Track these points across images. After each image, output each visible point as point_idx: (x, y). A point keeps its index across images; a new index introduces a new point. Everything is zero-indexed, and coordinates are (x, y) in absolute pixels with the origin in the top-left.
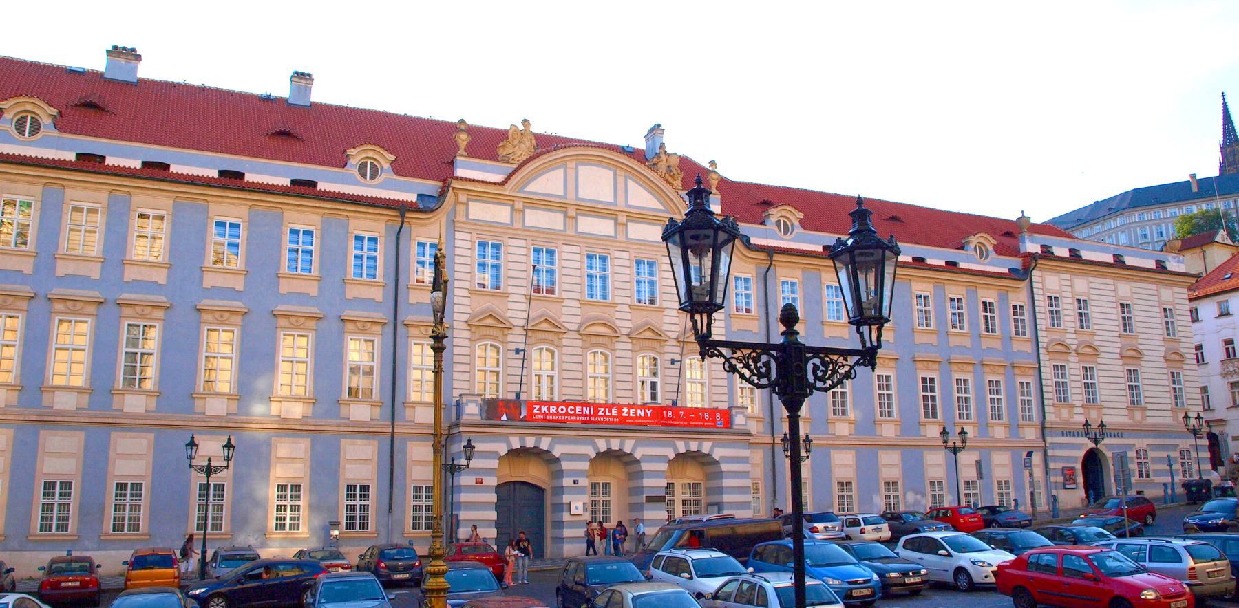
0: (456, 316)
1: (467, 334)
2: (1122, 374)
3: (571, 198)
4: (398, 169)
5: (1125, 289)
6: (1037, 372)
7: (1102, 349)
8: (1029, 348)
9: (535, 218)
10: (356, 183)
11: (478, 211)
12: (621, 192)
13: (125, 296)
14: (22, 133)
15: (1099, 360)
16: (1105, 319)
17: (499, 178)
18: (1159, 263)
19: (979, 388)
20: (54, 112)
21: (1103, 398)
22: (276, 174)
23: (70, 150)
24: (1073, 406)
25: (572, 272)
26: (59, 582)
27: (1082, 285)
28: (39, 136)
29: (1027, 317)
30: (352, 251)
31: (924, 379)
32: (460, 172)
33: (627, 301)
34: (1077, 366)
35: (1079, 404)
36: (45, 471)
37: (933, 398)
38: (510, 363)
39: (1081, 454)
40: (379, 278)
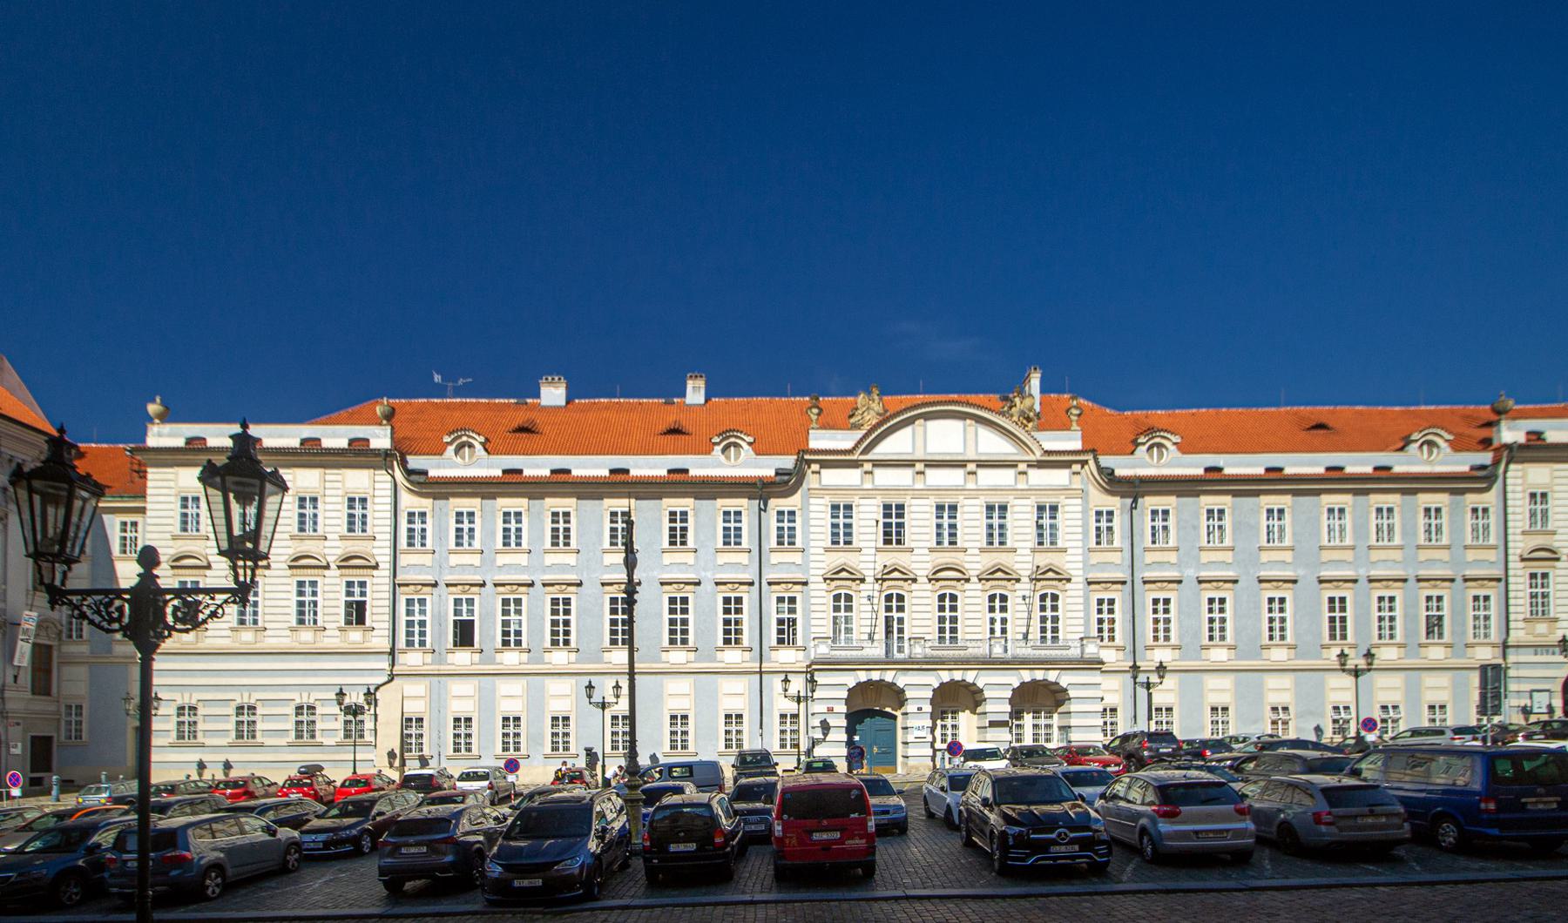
0: (812, 572)
1: (824, 586)
3: (919, 455)
4: (760, 449)
9: (884, 477)
10: (720, 465)
11: (831, 477)
12: (971, 443)
17: (849, 445)
19: (1410, 605)
20: (482, 439)
22: (654, 467)
25: (921, 523)
30: (721, 525)
32: (813, 444)
33: (978, 545)
37: (1343, 619)
38: (863, 608)
40: (745, 544)
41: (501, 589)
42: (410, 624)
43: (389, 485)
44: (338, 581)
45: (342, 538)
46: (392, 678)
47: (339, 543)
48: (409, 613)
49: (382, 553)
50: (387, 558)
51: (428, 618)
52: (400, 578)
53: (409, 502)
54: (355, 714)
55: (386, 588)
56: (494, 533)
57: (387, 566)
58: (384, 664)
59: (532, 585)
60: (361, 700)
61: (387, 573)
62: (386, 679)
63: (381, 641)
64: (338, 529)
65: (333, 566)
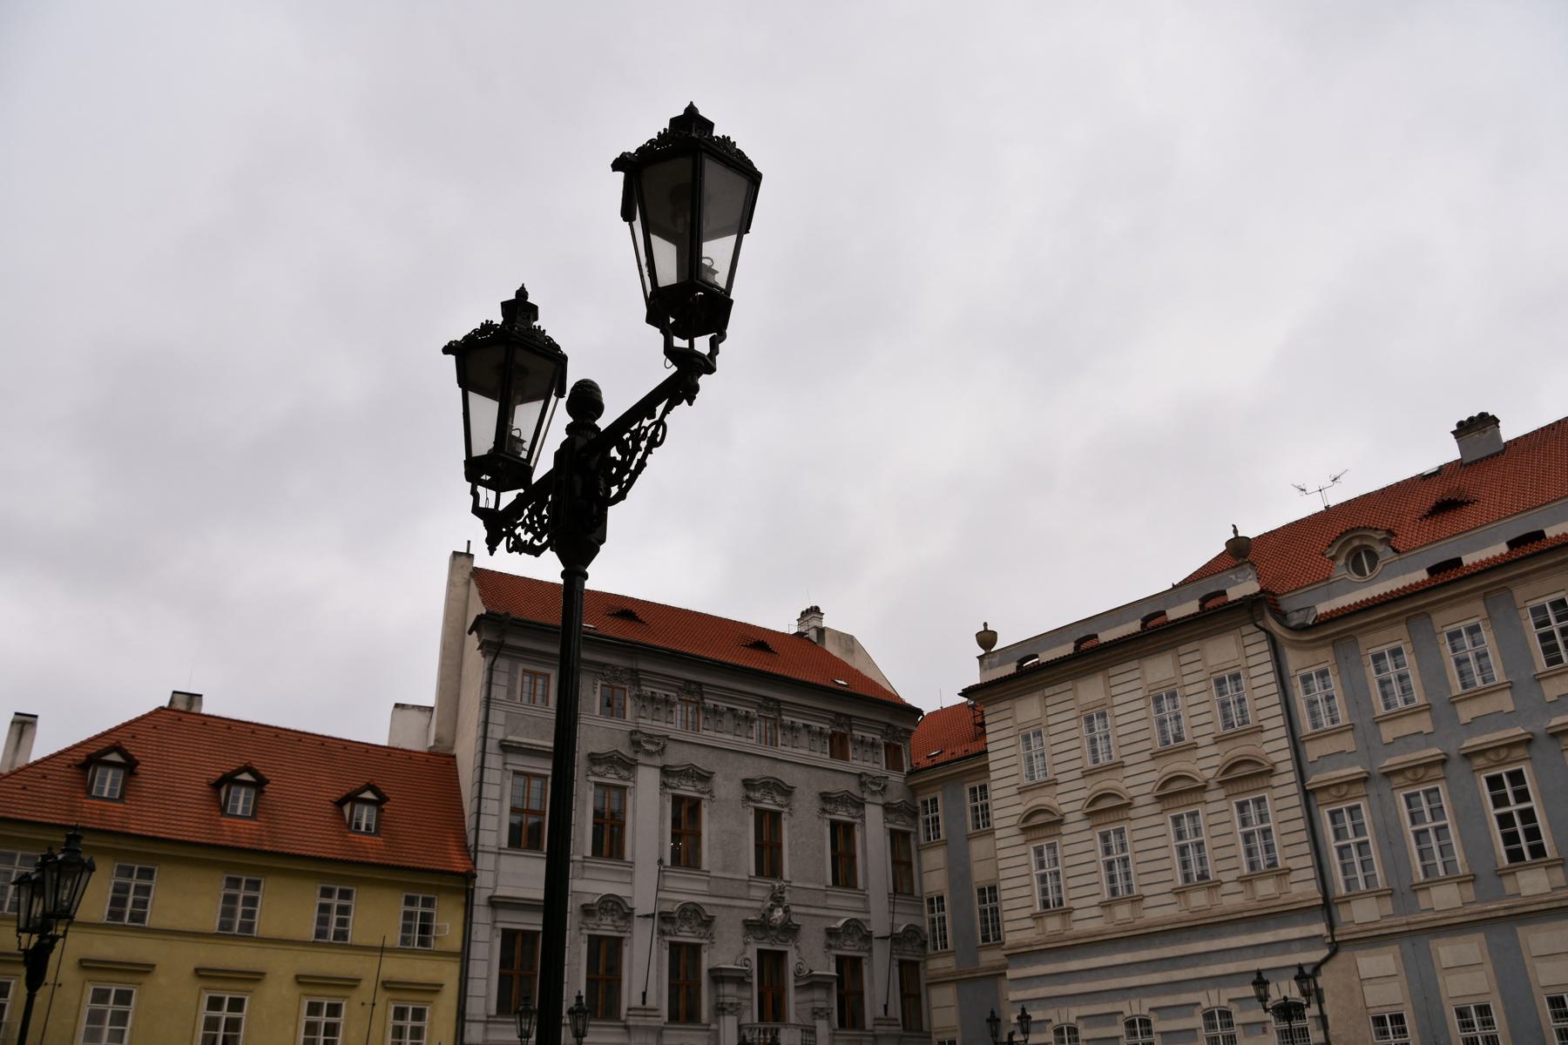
13: (1555, 722)
14: (1361, 573)
23: (1418, 568)
28: (1379, 567)
36: (1543, 982)
41: (1480, 762)
42: (1343, 851)
43: (1265, 646)
44: (1222, 805)
45: (1218, 740)
46: (1335, 948)
47: (1214, 750)
48: (1339, 834)
49: (1274, 747)
50: (1287, 754)
51: (1369, 837)
52: (1314, 780)
53: (1295, 661)
54: (1289, 1018)
55: (1296, 800)
56: (1442, 673)
57: (1289, 766)
58: (1320, 928)
59: (1528, 742)
60: (1295, 993)
61: (1291, 777)
62: (1326, 952)
63: (1304, 888)
64: (1209, 728)
65: (1213, 784)
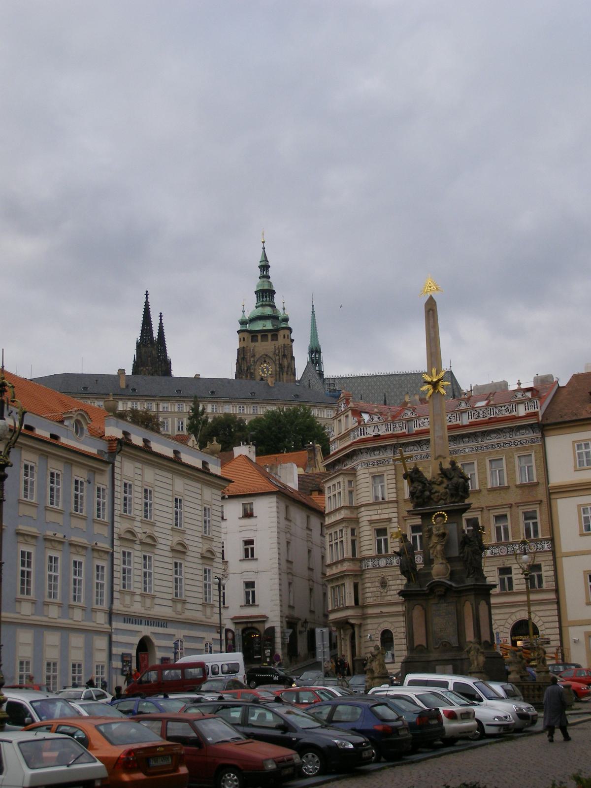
2: (170, 566)
5: (180, 485)
6: (108, 557)
7: (160, 540)
8: (105, 531)
15: (157, 551)
16: (163, 511)
18: (204, 463)
21: (157, 588)
24: (133, 594)
26: (141, 679)
27: (151, 475)
29: (107, 500)
31: (23, 553)
34: (137, 554)
35: (138, 591)
37: (29, 573)
39: (136, 640)
